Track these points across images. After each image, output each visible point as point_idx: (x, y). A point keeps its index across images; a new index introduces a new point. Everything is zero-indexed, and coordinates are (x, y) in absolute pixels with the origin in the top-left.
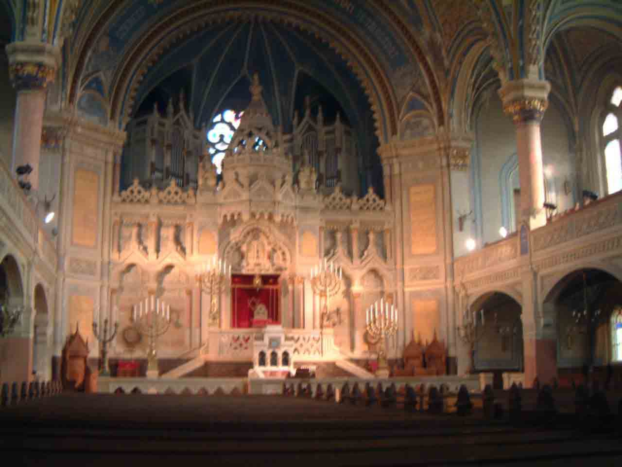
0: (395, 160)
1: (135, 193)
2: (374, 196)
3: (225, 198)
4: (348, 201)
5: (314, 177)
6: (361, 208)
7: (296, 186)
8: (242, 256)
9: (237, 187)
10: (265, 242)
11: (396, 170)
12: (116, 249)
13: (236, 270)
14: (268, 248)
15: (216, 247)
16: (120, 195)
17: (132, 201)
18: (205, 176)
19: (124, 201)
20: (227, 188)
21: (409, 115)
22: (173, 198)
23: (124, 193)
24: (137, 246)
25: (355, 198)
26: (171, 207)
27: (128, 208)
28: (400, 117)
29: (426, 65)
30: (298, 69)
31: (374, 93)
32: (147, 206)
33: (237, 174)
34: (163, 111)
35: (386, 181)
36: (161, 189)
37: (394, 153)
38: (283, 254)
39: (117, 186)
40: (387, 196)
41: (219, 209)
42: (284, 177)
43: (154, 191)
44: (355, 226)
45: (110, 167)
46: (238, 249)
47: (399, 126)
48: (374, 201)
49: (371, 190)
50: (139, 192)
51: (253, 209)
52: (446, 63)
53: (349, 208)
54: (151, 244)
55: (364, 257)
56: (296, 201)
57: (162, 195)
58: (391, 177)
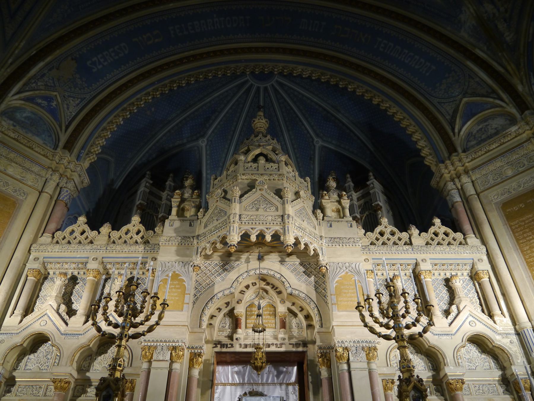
0: (465, 179)
1: (77, 234)
2: (444, 229)
3: (206, 226)
4: (404, 235)
5: (346, 203)
6: (427, 244)
7: (319, 211)
8: (236, 324)
9: (222, 205)
10: (277, 299)
11: (470, 190)
12: (19, 310)
13: (223, 346)
14: (282, 309)
15: (189, 299)
16: (53, 237)
17: (69, 242)
18: (182, 206)
19: (57, 242)
20: (210, 211)
21: (469, 123)
22: (132, 238)
23: (58, 233)
24: (55, 306)
25: (415, 231)
26: (126, 248)
27: (56, 251)
28: (456, 130)
29: (477, 60)
30: (319, 143)
31: (413, 123)
32: (89, 247)
33: (225, 192)
34: (159, 183)
35: (461, 208)
36: (116, 227)
37: (460, 169)
38: (308, 317)
39: (52, 226)
40: (467, 227)
41: (195, 241)
42: (297, 194)
43: (106, 229)
44: (423, 267)
45: (45, 197)
46: (231, 314)
47: (458, 141)
48: (446, 234)
49: (437, 221)
50: (83, 233)
51: (246, 228)
52: (509, 37)
53: (411, 244)
54: (81, 304)
55: (451, 317)
56: (323, 230)
57: (115, 234)
58: (466, 200)
